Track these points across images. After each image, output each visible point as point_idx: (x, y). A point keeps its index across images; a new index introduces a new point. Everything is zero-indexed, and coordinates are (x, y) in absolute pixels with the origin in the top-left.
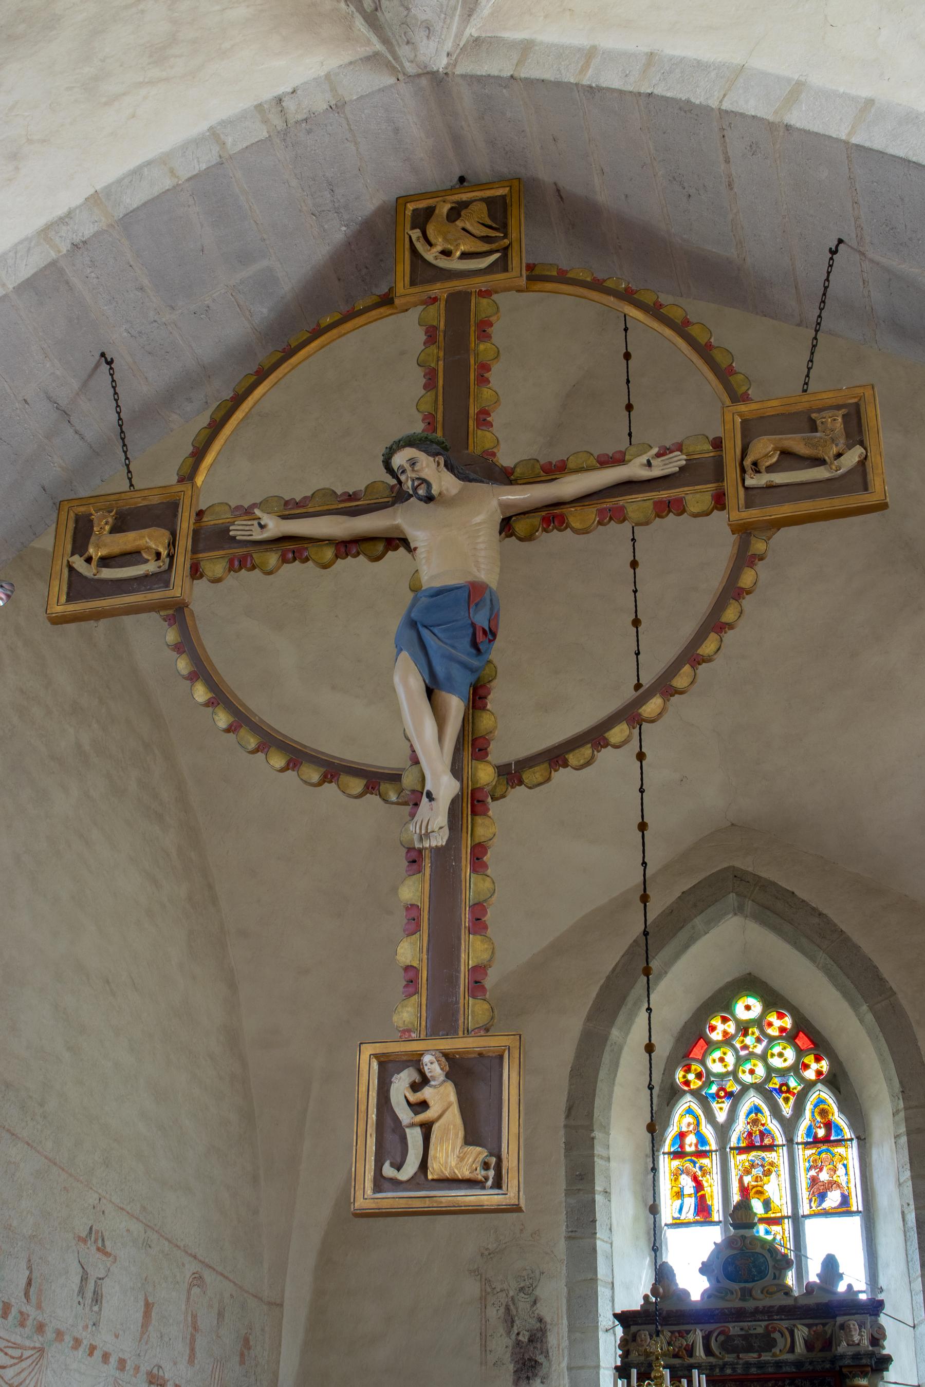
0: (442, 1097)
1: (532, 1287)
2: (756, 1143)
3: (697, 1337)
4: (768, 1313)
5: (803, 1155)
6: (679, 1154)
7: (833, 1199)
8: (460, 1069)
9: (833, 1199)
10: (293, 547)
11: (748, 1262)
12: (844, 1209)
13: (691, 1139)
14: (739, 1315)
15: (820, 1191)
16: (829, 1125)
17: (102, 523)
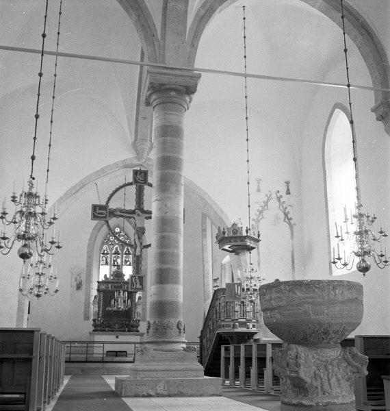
0: (138, 281)
1: (81, 274)
2: (116, 253)
3: (110, 285)
4: (120, 283)
5: (124, 256)
6: (103, 254)
7: (128, 263)
8: (139, 277)
9: (128, 263)
10: (121, 216)
11: (118, 275)
12: (130, 265)
13: (106, 252)
14: (117, 283)
15: (126, 262)
16: (129, 252)
17: (98, 208)
